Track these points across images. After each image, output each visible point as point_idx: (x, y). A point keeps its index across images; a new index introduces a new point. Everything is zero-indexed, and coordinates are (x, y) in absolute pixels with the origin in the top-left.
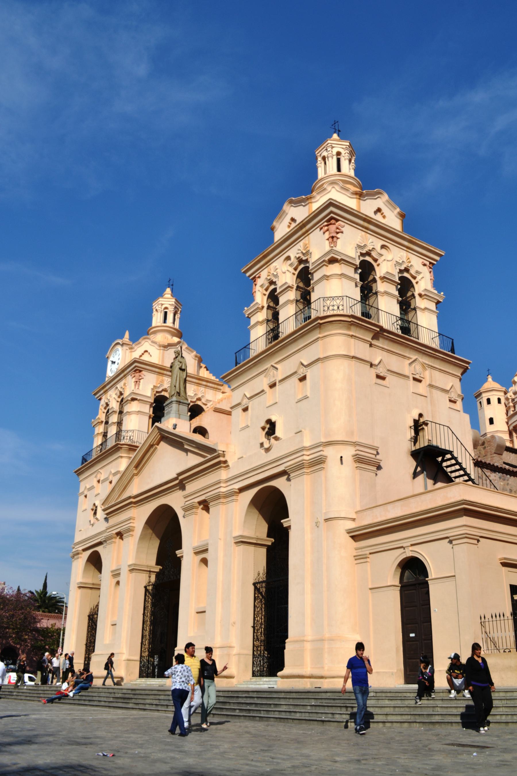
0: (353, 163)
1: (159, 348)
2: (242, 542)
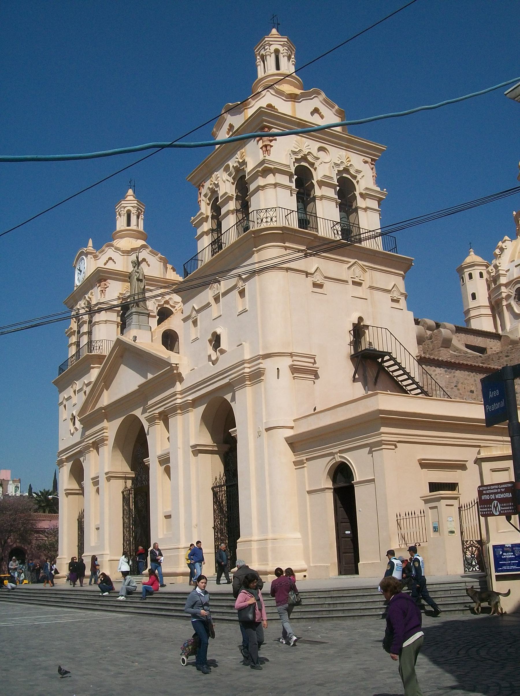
0: (293, 58)
2: (197, 450)
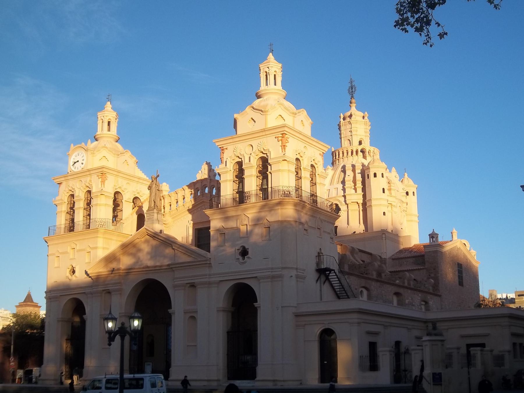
1: (114, 156)
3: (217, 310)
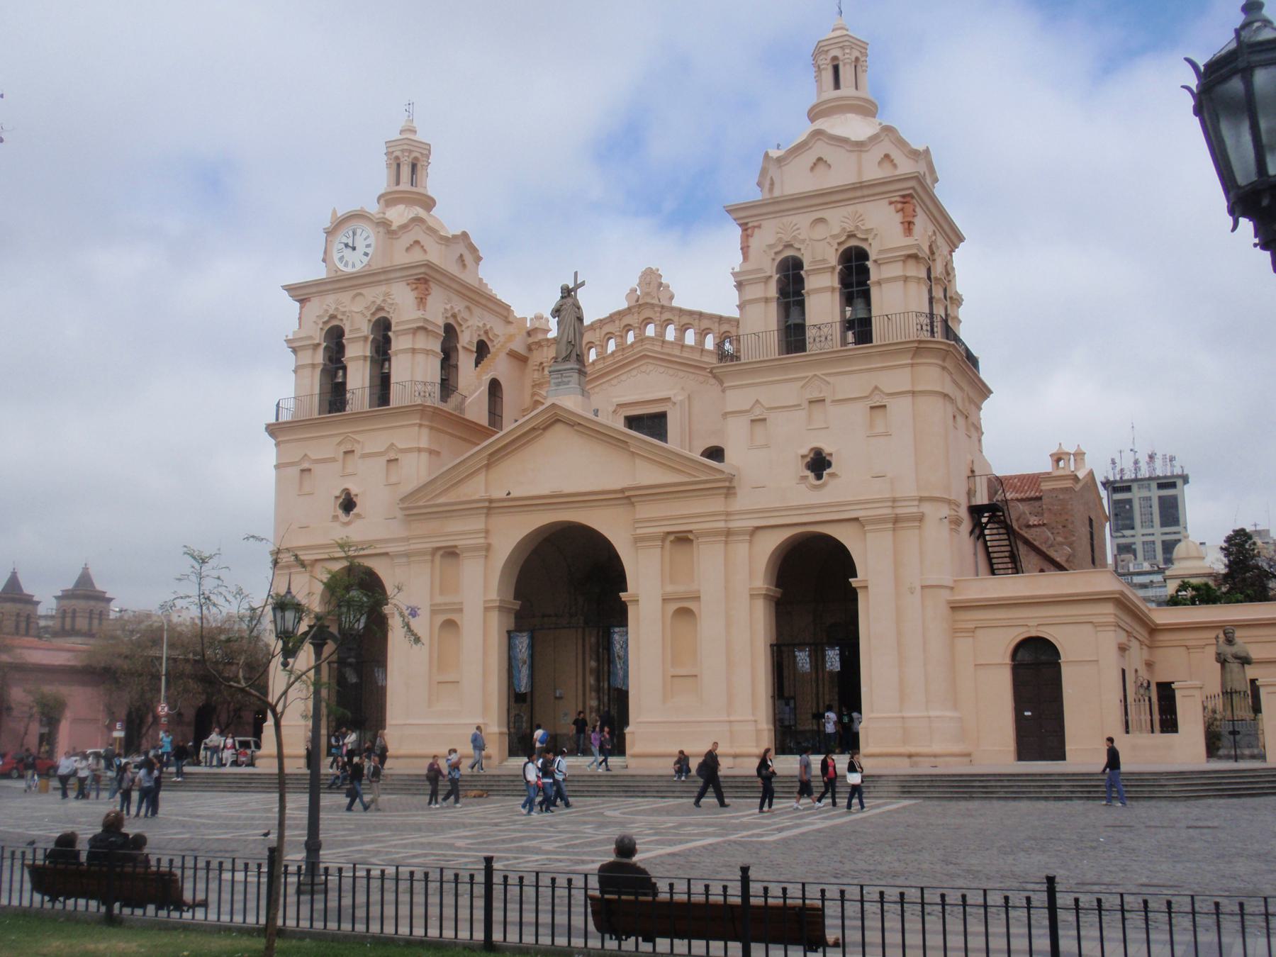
3: (751, 595)
